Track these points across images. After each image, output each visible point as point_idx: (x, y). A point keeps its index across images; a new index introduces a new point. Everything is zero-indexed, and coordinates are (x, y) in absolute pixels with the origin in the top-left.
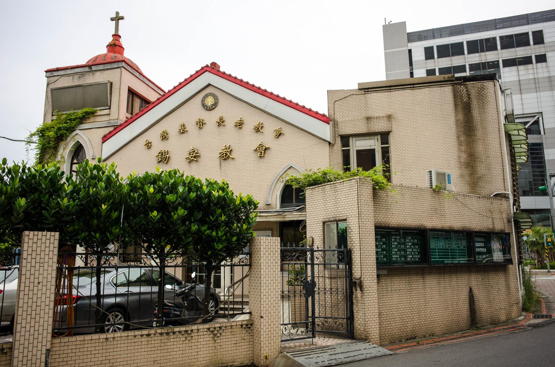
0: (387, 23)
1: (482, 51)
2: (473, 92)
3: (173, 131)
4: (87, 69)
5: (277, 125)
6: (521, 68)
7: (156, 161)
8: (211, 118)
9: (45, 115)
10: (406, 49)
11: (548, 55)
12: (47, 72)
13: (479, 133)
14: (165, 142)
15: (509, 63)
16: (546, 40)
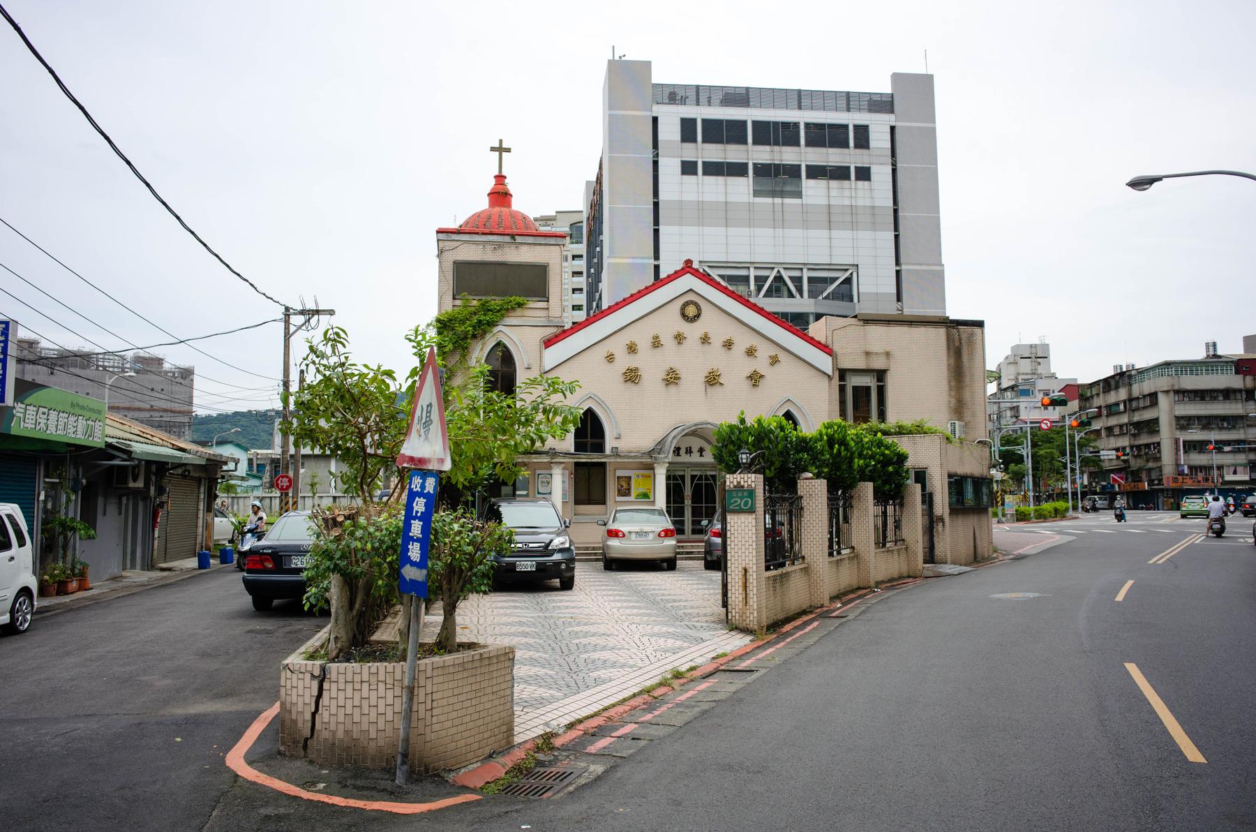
0: (617, 58)
1: (776, 143)
2: (964, 337)
3: (644, 344)
4: (507, 239)
5: (773, 351)
6: (834, 183)
7: (622, 379)
8: (693, 331)
9: (440, 298)
10: (649, 115)
11: (874, 170)
12: (438, 232)
13: (967, 379)
14: (632, 356)
15: (816, 172)
16: (872, 144)
